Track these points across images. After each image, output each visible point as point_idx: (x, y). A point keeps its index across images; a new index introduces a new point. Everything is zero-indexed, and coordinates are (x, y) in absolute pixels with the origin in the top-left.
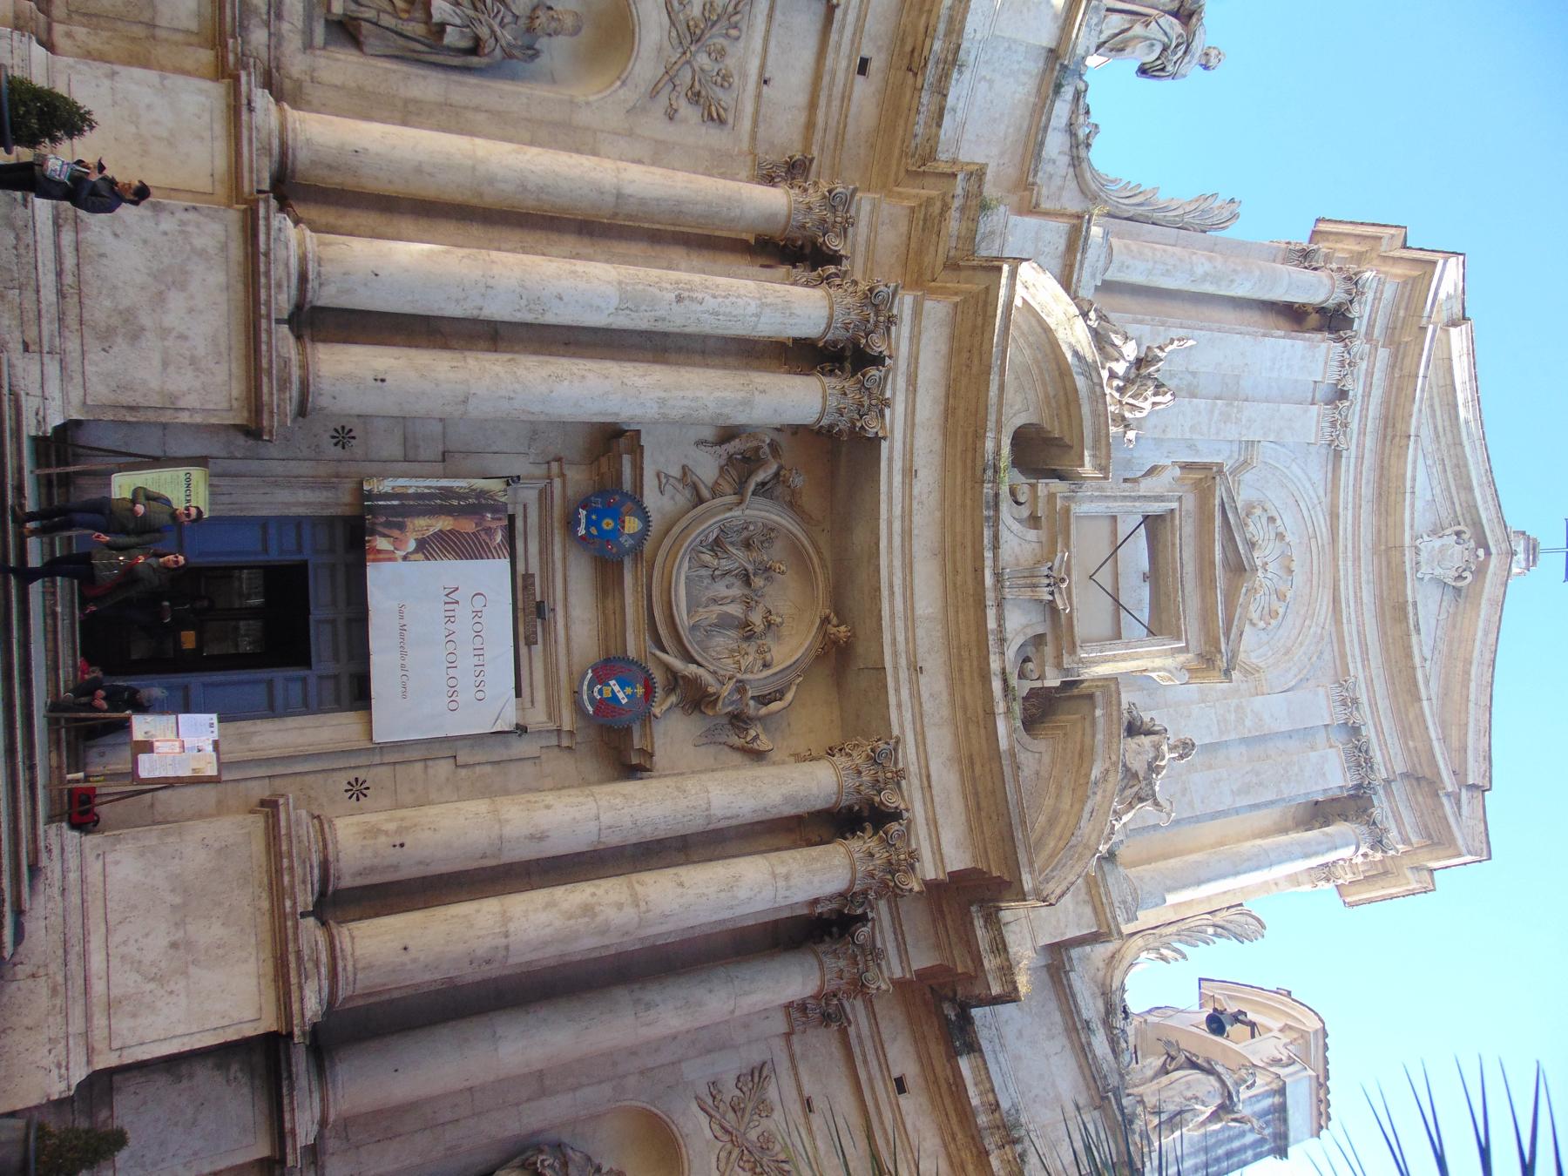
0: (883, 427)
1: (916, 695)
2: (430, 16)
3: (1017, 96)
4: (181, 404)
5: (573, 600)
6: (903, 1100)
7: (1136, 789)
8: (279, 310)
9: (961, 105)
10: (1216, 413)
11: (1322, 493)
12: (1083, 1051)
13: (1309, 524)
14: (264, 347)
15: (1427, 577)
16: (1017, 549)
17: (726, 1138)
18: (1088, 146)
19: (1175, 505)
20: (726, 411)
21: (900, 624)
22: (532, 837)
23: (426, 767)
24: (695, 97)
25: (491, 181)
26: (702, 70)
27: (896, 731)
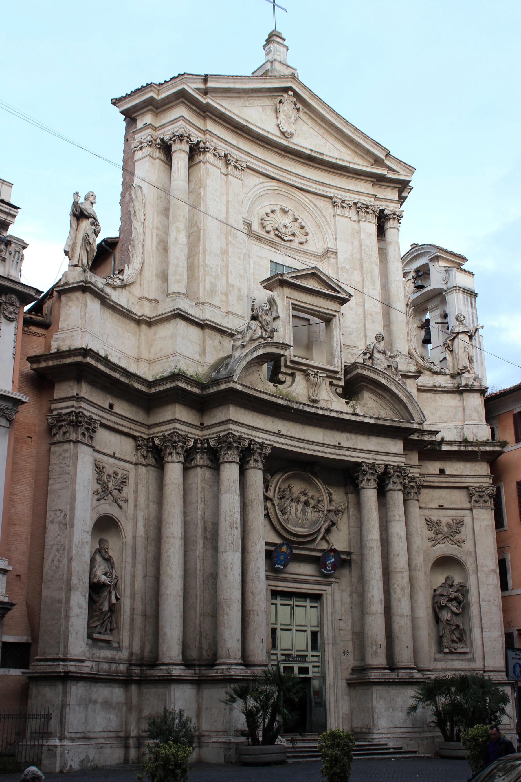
0: (269, 445)
5: (297, 571)
6: (447, 472)
7: (393, 368)
9: (117, 354)
10: (233, 242)
12: (444, 391)
13: (269, 192)
17: (445, 539)
23: (341, 630)
27: (360, 460)
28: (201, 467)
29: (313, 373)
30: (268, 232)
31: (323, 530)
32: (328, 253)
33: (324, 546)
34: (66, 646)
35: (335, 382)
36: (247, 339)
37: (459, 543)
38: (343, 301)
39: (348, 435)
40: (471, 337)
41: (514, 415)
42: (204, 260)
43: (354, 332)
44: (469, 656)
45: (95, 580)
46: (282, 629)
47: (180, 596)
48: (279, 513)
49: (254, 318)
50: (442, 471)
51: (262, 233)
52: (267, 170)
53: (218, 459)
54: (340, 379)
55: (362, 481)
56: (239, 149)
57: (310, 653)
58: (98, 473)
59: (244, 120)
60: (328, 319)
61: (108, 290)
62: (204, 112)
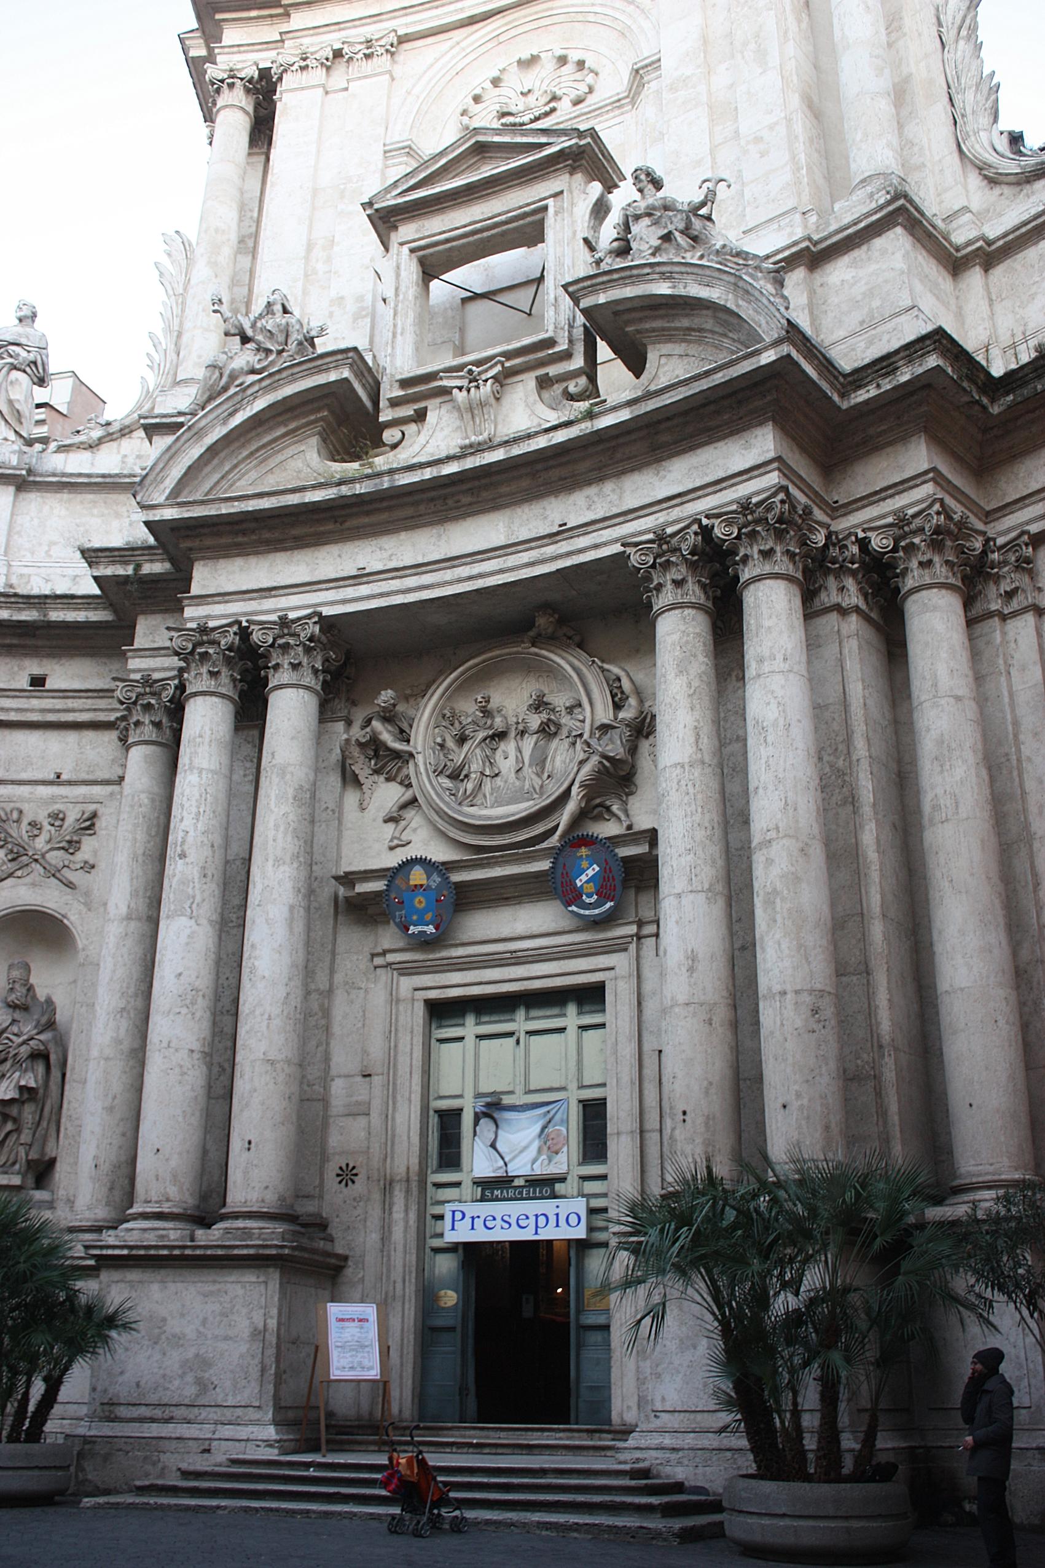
0: (309, 617)
2: (12, 1101)
3: (63, 512)
4: (261, 1326)
5: (506, 932)
7: (677, 234)
8: (182, 1238)
11: (450, 43)
14: (209, 1252)
16: (446, 432)
18: (108, 424)
19: (405, 249)
20: (291, 792)
21: (512, 561)
22: (691, 970)
24: (72, 846)
25: (118, 1041)
26: (49, 842)
27: (617, 548)
29: (464, 383)
35: (553, 370)
47: (107, 1059)
52: (462, 10)
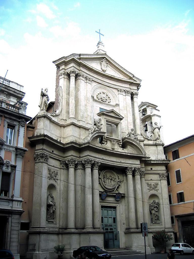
1: (124, 163)
15: (106, 69)
21: (117, 163)
27: (127, 166)
28: (80, 169)
30: (99, 99)
31: (116, 187)
32: (117, 105)
33: (117, 192)
34: (40, 224)
35: (119, 143)
36: (93, 131)
37: (157, 190)
38: (121, 119)
39: (123, 159)
40: (159, 129)
41: (172, 152)
42: (80, 108)
43: (125, 128)
44: (161, 224)
45: (49, 204)
46: (104, 217)
48: (103, 183)
49: (95, 125)
50: (151, 169)
51: (97, 99)
53: (85, 167)
54: (121, 142)
55: (128, 172)
56: (90, 75)
57: (113, 224)
58: (49, 171)
59: (91, 67)
60: (117, 125)
61: (51, 117)
62: (80, 65)
